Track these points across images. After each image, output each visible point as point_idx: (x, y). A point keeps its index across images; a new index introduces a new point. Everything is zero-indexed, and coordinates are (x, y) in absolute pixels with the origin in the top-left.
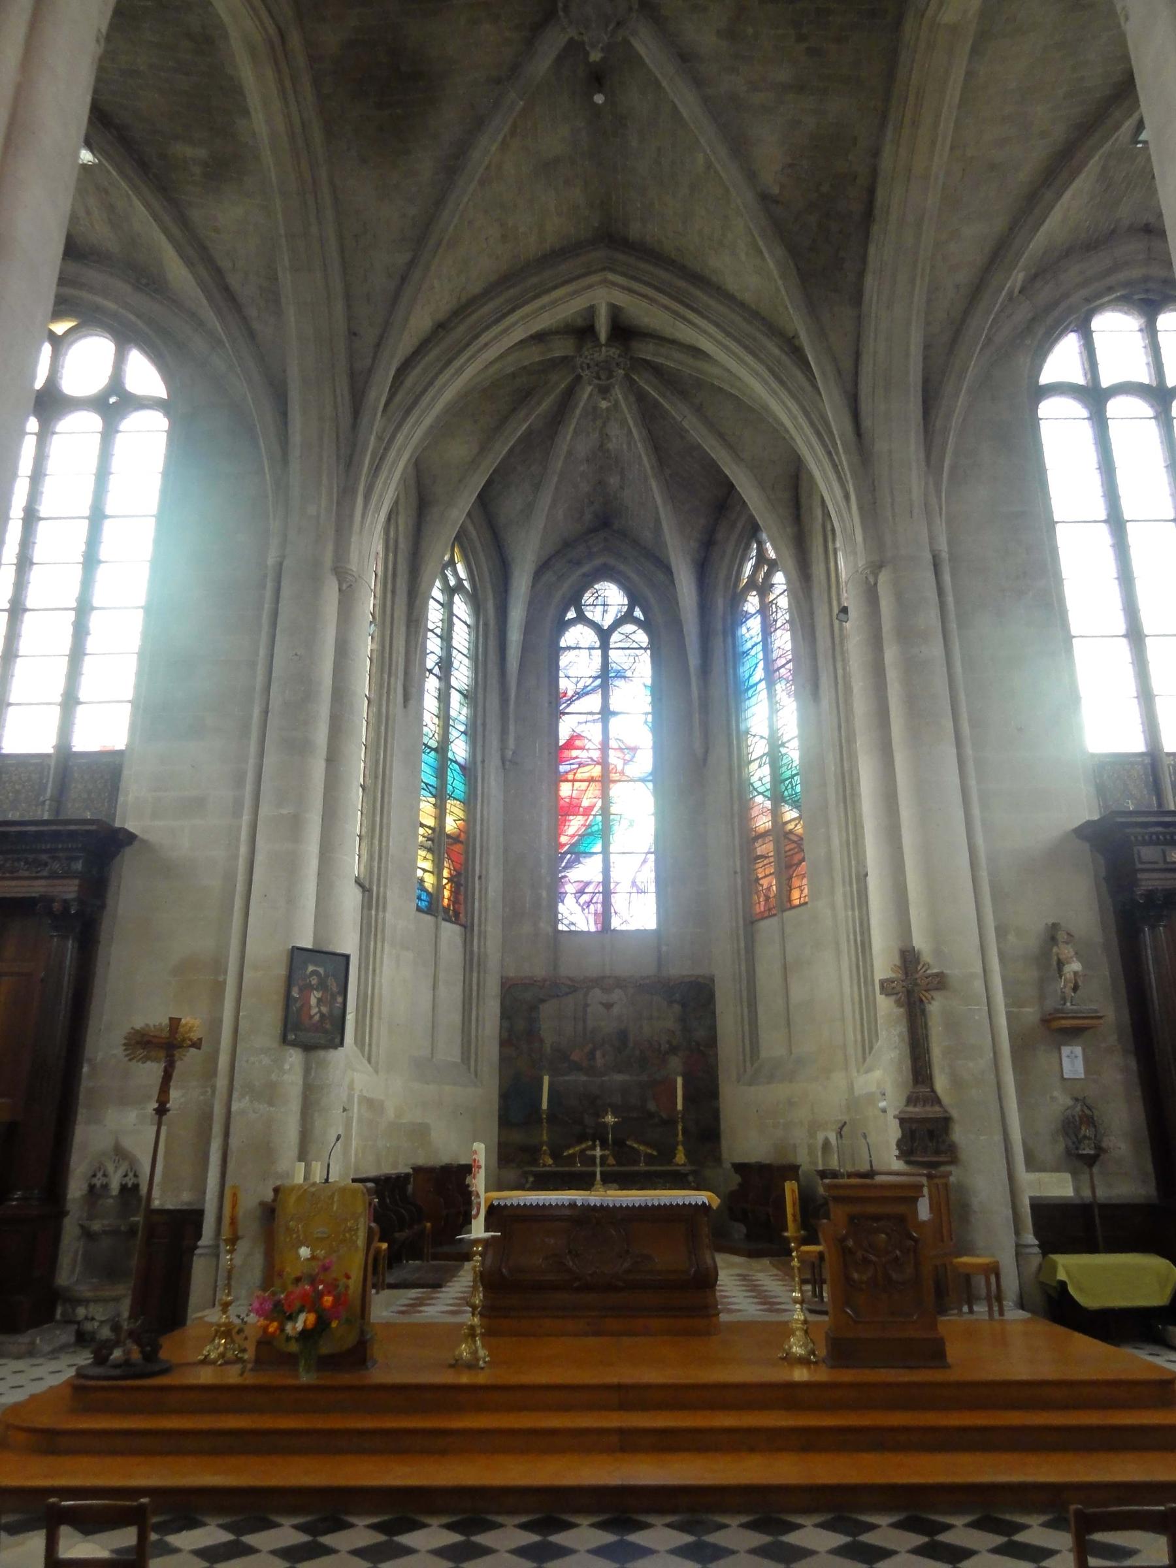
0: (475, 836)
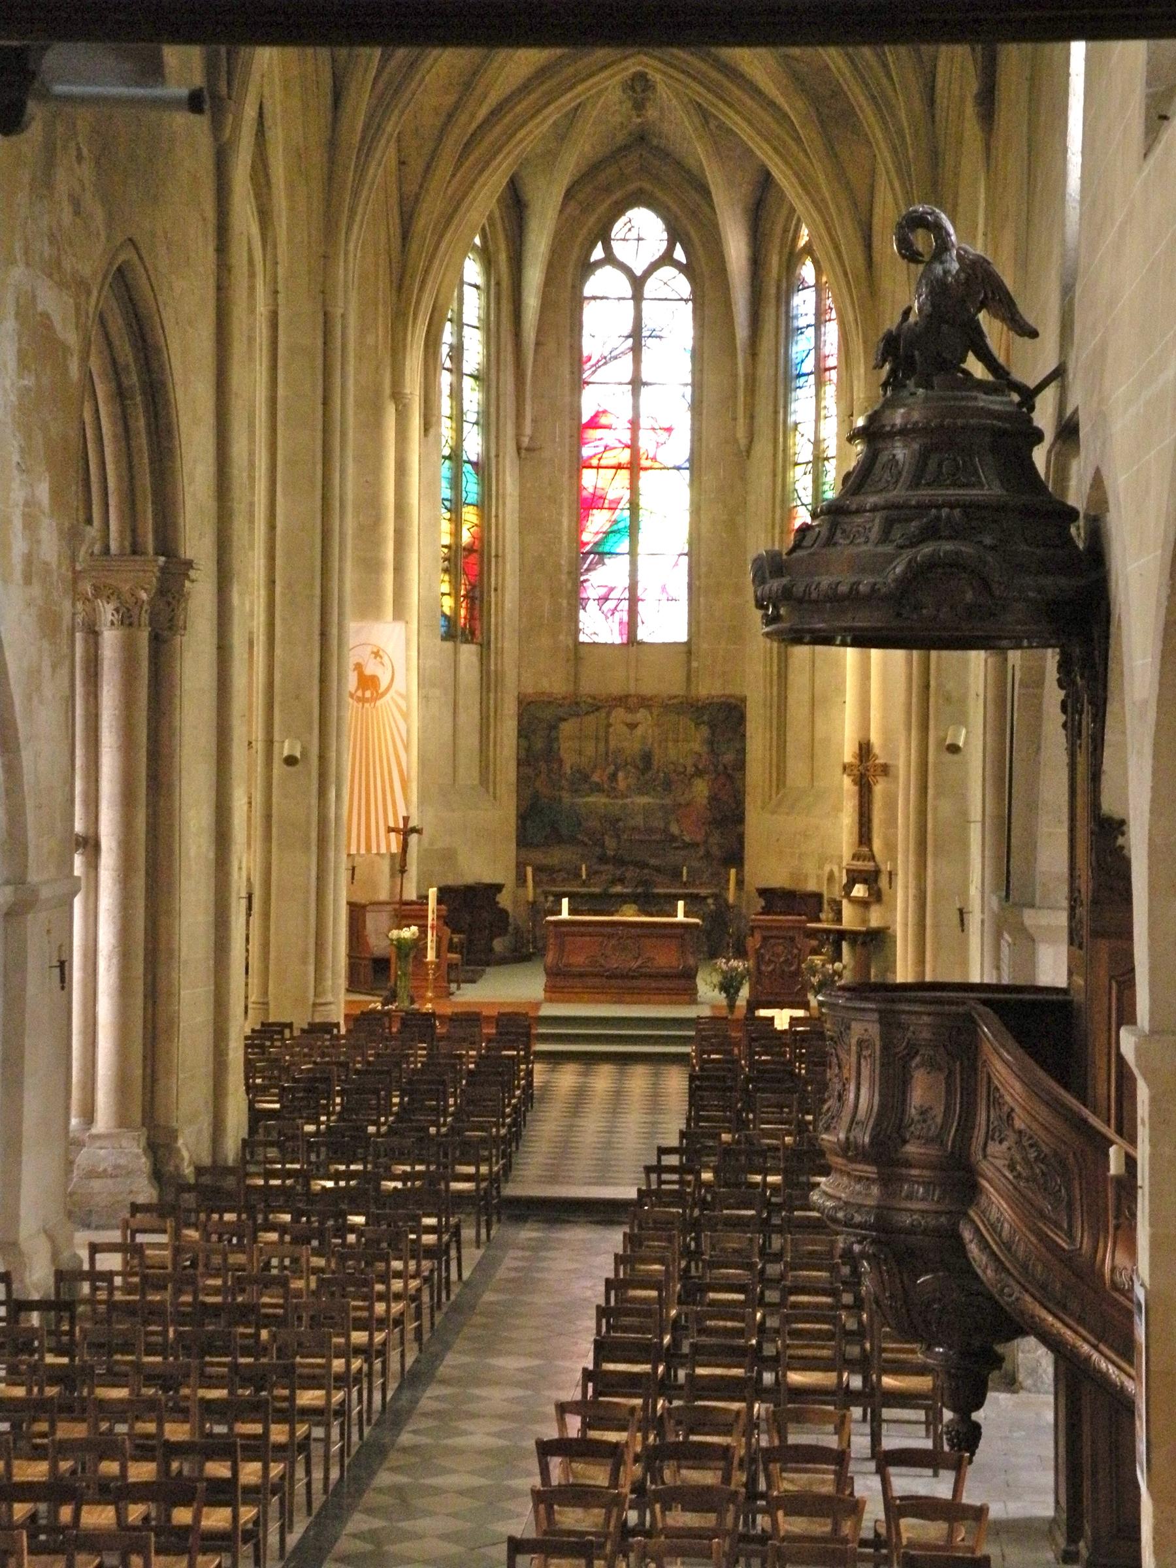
0: (489, 542)
